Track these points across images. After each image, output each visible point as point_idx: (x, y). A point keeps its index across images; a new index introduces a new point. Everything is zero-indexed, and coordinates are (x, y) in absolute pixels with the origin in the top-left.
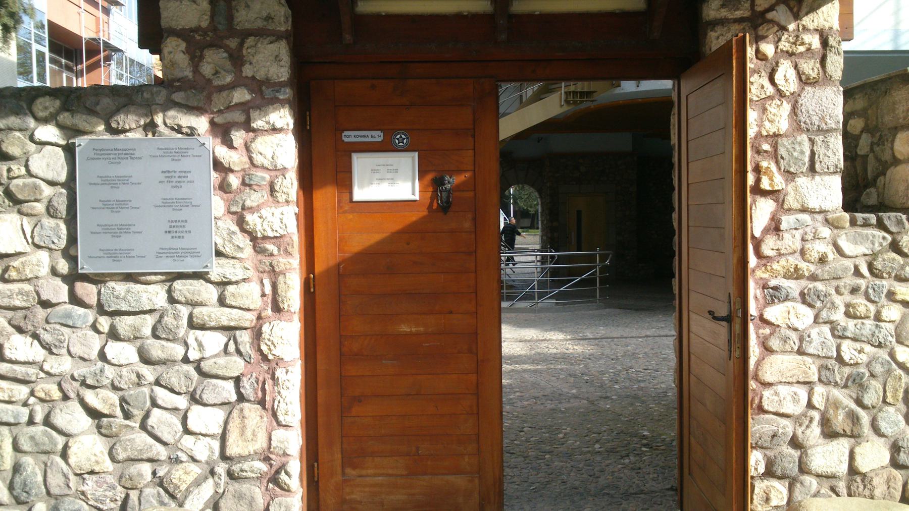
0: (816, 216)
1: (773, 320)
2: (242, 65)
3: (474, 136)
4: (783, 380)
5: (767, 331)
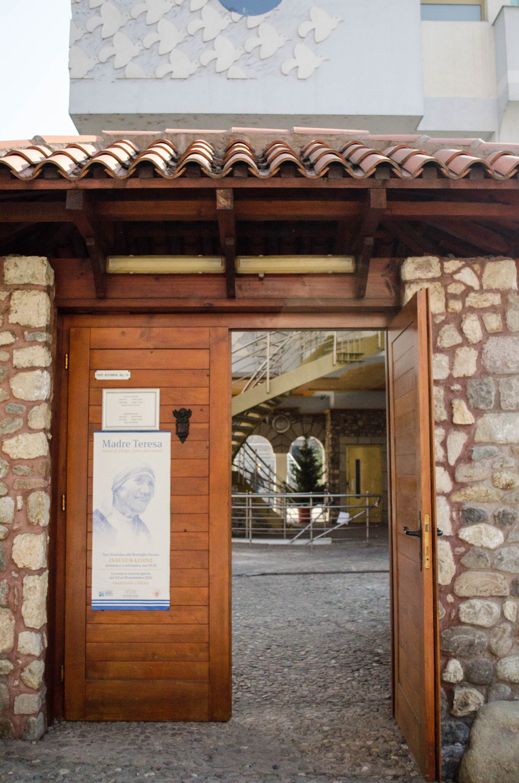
0: (504, 448)
1: (467, 539)
2: (9, 314)
3: (209, 376)
4: (478, 594)
5: (462, 550)
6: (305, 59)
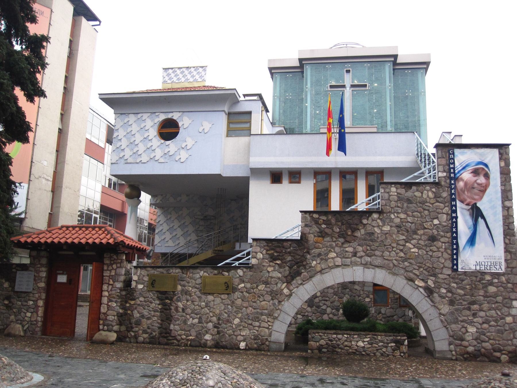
6: (183, 155)
